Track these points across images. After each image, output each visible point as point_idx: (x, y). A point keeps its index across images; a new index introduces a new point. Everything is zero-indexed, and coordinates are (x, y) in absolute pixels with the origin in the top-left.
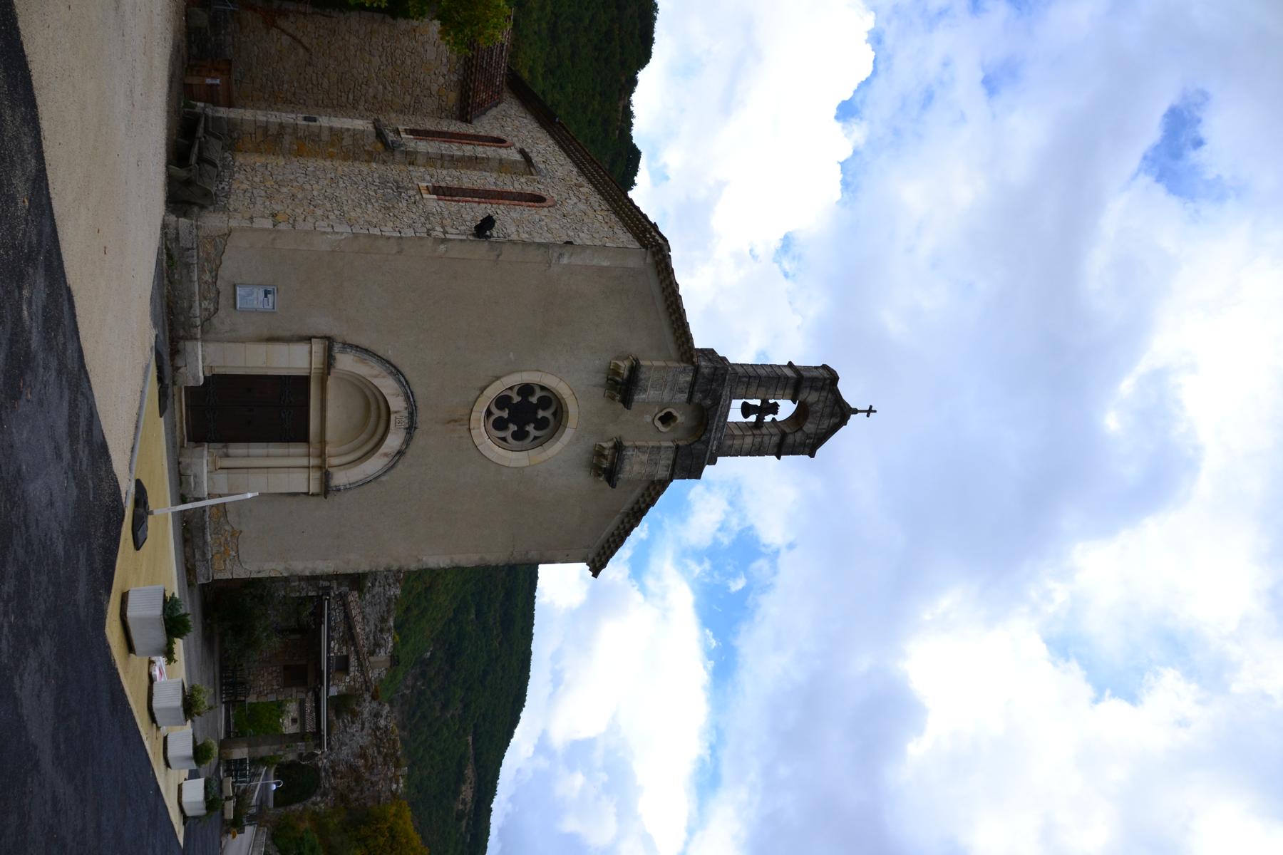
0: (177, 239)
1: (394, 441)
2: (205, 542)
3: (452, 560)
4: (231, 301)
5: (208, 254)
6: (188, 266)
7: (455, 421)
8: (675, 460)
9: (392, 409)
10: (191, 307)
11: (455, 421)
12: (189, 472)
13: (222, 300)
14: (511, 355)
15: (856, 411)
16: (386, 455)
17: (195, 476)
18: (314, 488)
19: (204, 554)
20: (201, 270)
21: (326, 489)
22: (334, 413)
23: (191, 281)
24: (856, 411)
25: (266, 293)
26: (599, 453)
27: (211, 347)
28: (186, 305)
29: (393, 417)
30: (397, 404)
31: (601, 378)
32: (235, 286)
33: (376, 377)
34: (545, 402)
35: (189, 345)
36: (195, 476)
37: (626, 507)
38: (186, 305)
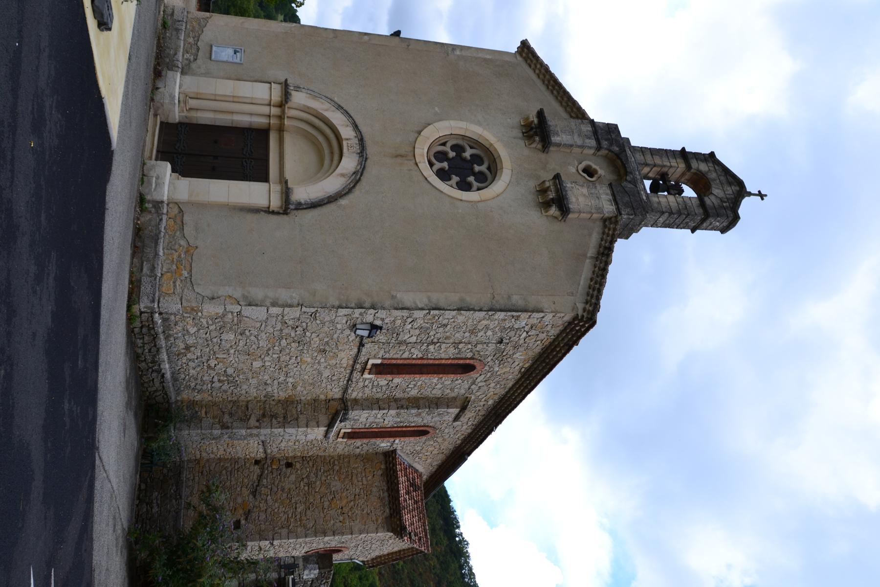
0: (172, 14)
1: (349, 163)
2: (156, 254)
3: (429, 299)
4: (208, 55)
5: (193, 27)
6: (178, 30)
7: (402, 156)
8: (613, 195)
9: (344, 136)
10: (176, 54)
11: (402, 156)
12: (152, 173)
13: (200, 54)
14: (437, 109)
15: (750, 194)
16: (343, 175)
17: (158, 178)
18: (276, 203)
19: (153, 269)
20: (187, 36)
21: (285, 85)
22: (292, 157)
23: (178, 38)
24: (750, 194)
25: (235, 52)
26: (542, 191)
27: (188, 79)
28: (172, 52)
29: (345, 143)
30: (347, 132)
31: (517, 133)
32: (211, 46)
33: (326, 110)
34: (477, 159)
35: (170, 74)
36: (158, 178)
37: (591, 252)
38: (172, 52)
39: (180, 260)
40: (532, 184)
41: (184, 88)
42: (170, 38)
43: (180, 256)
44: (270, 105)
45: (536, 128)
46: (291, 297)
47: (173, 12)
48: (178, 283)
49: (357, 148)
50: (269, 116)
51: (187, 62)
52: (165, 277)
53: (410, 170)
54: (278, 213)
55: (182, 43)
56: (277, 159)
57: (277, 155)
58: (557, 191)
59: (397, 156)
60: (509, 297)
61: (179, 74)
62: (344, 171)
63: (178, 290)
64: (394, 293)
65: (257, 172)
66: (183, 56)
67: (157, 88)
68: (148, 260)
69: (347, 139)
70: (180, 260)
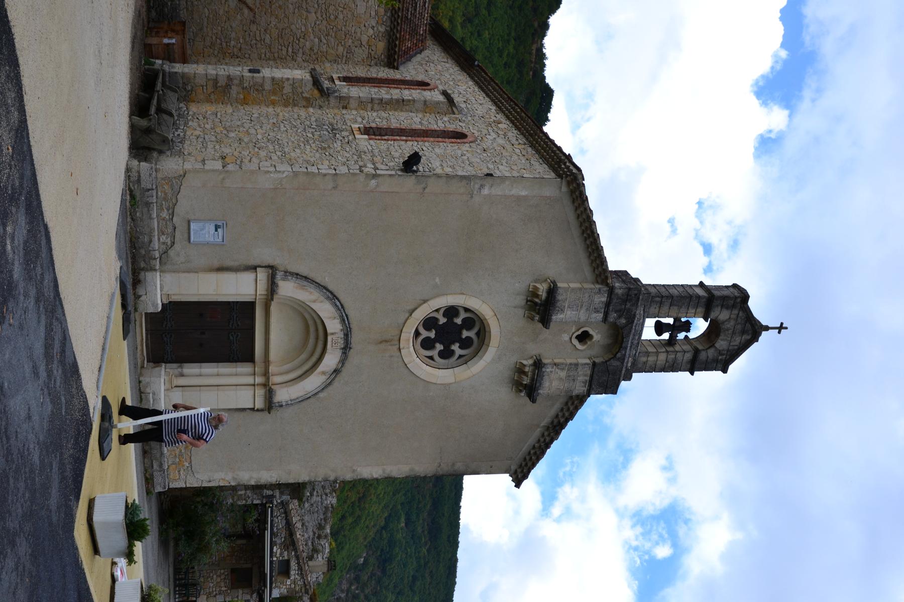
0: (139, 181)
1: (331, 360)
2: (162, 454)
3: (384, 471)
4: (186, 235)
5: (166, 194)
6: (148, 204)
7: (386, 341)
8: (592, 377)
9: (329, 331)
10: (151, 241)
11: (386, 341)
12: (148, 390)
13: (178, 234)
14: (437, 280)
15: (767, 328)
16: (324, 373)
17: (154, 394)
18: (259, 404)
19: (161, 465)
20: (160, 209)
21: (270, 405)
22: (277, 335)
23: (151, 218)
24: (767, 328)
25: (217, 227)
26: (520, 370)
27: (168, 277)
28: (146, 239)
29: (329, 338)
30: (334, 326)
31: (521, 300)
32: (189, 222)
33: (314, 301)
34: (469, 323)
35: (149, 275)
36: (154, 394)
37: (545, 422)
38: (146, 239)
39: (181, 454)
40: (513, 359)
41: (165, 289)
42: (142, 220)
43: (181, 451)
44: (254, 385)
45: (541, 305)
46: (271, 477)
47: (139, 176)
48: (182, 472)
49: (341, 343)
50: (254, 385)
51: (164, 247)
52: (171, 468)
53: (391, 356)
54: (262, 410)
55: (155, 221)
56: (263, 330)
57: (263, 325)
58: (533, 379)
59: (381, 342)
60: (453, 464)
61: (158, 274)
62: (324, 369)
63: (183, 476)
64: (355, 468)
65: (243, 352)
66: (159, 239)
67: (140, 296)
68: (156, 459)
69: (332, 334)
70: (181, 454)
